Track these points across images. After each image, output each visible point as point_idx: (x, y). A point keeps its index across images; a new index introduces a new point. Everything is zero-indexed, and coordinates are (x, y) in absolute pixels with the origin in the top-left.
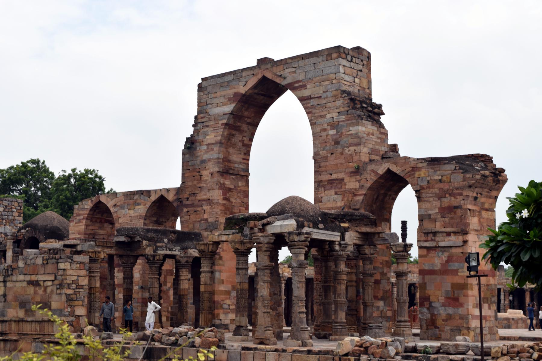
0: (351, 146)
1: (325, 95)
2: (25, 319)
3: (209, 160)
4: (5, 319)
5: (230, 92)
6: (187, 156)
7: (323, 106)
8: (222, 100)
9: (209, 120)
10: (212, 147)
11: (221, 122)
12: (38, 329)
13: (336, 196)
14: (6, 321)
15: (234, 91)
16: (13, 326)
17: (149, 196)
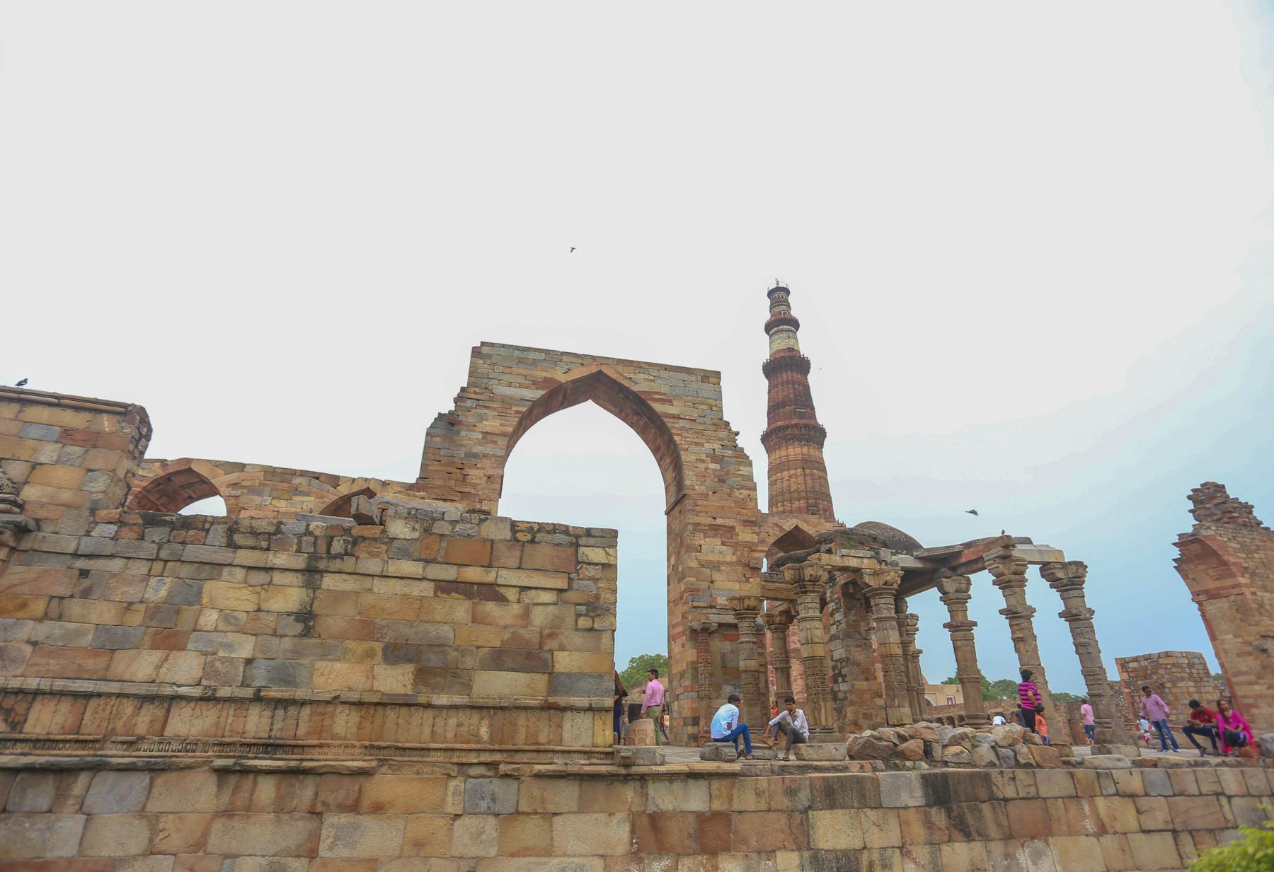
0: (742, 488)
1: (701, 420)
2: (422, 699)
3: (485, 456)
4: (300, 693)
5: (541, 374)
6: (438, 439)
7: (700, 433)
8: (520, 380)
9: (491, 399)
10: (495, 438)
11: (514, 408)
12: (484, 731)
13: (724, 548)
14: (303, 703)
15: (545, 374)
16: (344, 721)
17: (336, 486)
